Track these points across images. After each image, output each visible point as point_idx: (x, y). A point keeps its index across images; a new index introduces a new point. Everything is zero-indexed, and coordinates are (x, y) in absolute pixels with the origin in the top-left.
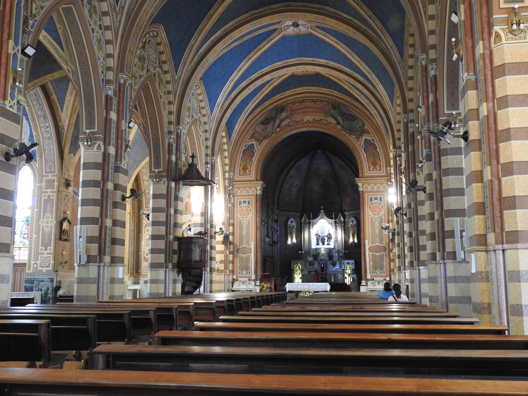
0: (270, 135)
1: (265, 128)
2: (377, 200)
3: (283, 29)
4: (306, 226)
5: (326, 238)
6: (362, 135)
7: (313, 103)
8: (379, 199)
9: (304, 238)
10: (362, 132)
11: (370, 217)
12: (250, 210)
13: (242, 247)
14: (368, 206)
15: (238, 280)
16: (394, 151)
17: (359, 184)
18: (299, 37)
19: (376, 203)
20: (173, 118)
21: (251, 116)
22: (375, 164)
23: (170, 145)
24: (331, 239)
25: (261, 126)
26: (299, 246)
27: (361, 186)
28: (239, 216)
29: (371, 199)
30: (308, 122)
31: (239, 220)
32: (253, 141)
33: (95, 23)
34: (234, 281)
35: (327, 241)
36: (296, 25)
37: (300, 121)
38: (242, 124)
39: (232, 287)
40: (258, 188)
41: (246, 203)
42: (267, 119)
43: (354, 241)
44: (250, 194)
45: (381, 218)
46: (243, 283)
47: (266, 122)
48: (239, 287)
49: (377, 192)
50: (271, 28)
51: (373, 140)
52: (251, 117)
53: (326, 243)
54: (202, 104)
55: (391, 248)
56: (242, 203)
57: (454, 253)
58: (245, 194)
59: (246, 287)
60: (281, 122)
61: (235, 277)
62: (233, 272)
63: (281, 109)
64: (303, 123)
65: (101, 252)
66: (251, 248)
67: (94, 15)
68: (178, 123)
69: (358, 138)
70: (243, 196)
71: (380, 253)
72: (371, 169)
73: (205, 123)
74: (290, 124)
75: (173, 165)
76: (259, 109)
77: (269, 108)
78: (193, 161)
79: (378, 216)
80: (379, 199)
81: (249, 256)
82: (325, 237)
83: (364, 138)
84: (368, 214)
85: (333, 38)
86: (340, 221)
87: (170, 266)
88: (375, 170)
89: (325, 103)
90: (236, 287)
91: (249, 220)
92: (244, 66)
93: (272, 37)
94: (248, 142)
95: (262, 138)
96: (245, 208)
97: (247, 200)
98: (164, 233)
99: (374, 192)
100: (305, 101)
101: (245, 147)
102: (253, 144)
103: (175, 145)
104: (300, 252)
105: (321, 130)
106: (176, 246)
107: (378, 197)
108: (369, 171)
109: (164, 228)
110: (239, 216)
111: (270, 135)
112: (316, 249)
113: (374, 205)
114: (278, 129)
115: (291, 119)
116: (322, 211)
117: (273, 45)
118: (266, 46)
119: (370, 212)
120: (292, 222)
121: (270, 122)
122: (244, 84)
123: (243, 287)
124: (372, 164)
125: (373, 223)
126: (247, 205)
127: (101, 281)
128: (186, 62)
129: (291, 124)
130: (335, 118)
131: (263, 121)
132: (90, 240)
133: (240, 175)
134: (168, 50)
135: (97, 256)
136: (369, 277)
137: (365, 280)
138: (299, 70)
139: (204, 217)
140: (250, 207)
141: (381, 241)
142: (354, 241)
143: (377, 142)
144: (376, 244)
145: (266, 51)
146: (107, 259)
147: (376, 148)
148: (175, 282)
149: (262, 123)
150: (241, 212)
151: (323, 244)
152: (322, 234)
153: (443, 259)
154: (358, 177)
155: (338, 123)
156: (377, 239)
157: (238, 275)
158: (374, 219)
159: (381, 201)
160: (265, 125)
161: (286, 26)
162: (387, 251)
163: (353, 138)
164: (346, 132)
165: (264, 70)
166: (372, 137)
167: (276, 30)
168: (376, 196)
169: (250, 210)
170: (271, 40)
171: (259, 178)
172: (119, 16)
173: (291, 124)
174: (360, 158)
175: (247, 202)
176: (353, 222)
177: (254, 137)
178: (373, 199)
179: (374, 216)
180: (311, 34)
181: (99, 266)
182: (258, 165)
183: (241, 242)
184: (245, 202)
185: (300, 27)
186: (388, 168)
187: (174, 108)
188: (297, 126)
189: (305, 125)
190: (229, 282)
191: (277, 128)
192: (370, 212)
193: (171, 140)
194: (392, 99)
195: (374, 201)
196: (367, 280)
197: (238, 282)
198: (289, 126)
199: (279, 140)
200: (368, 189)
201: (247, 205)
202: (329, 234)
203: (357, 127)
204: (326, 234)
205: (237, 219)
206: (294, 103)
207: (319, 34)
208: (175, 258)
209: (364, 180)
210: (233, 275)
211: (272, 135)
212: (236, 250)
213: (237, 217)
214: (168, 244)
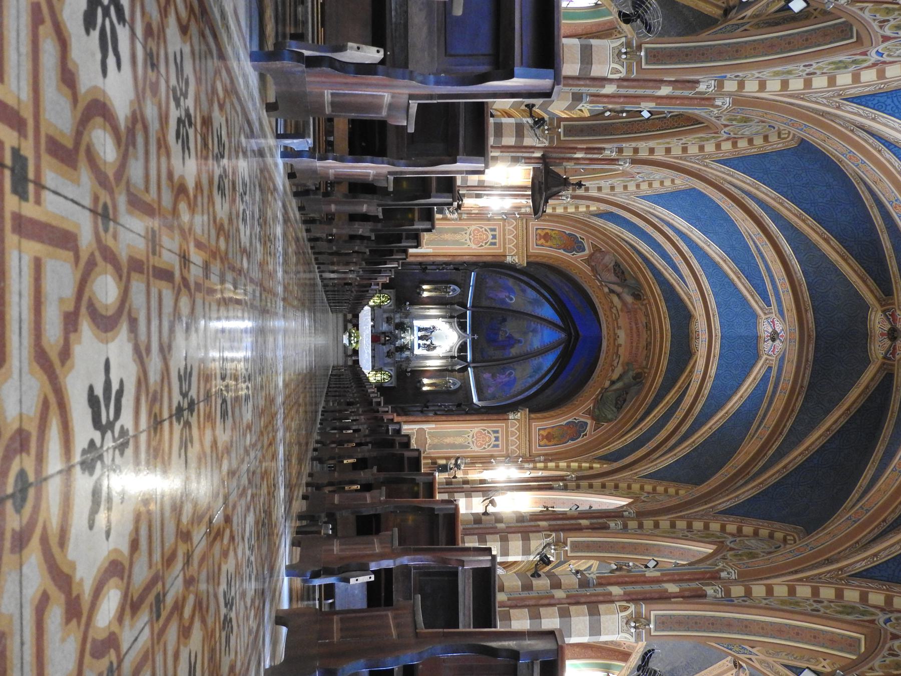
1: (609, 270)
2: (495, 441)
3: (768, 316)
4: (446, 312)
5: (428, 343)
6: (593, 418)
8: (497, 443)
9: (429, 309)
10: (598, 419)
11: (469, 430)
14: (485, 427)
16: (572, 477)
17: (519, 414)
18: (757, 338)
19: (490, 439)
21: (629, 247)
22: (549, 437)
24: (428, 350)
25: (613, 264)
26: (417, 300)
27: (516, 417)
29: (497, 432)
30: (616, 337)
35: (425, 344)
36: (774, 337)
38: (617, 235)
42: (623, 273)
45: (467, 447)
47: (619, 270)
49: (507, 440)
51: (586, 435)
52: (627, 248)
53: (421, 342)
60: (619, 295)
69: (589, 412)
72: (542, 432)
74: (614, 308)
79: (471, 443)
80: (497, 443)
82: (430, 341)
83: (589, 422)
84: (474, 427)
85: (750, 391)
86: (456, 365)
88: (540, 438)
93: (758, 297)
95: (593, 264)
99: (507, 436)
102: (584, 250)
104: (408, 303)
105: (603, 356)
107: (499, 443)
108: (539, 429)
112: (412, 328)
114: (606, 290)
115: (622, 310)
117: (744, 299)
118: (743, 286)
119: (476, 430)
121: (618, 277)
129: (614, 311)
130: (619, 379)
131: (619, 266)
149: (617, 265)
151: (420, 338)
152: (435, 337)
154: (531, 411)
158: (466, 436)
160: (615, 270)
161: (773, 322)
167: (769, 305)
170: (752, 296)
173: (614, 311)
174: (558, 416)
176: (454, 384)
178: (496, 435)
180: (757, 357)
185: (770, 342)
188: (610, 320)
189: (611, 333)
191: (609, 288)
192: (476, 430)
194: (651, 476)
195: (493, 436)
202: (435, 348)
203: (605, 410)
204: (435, 343)
207: (757, 371)
209: (525, 422)
211: (598, 280)
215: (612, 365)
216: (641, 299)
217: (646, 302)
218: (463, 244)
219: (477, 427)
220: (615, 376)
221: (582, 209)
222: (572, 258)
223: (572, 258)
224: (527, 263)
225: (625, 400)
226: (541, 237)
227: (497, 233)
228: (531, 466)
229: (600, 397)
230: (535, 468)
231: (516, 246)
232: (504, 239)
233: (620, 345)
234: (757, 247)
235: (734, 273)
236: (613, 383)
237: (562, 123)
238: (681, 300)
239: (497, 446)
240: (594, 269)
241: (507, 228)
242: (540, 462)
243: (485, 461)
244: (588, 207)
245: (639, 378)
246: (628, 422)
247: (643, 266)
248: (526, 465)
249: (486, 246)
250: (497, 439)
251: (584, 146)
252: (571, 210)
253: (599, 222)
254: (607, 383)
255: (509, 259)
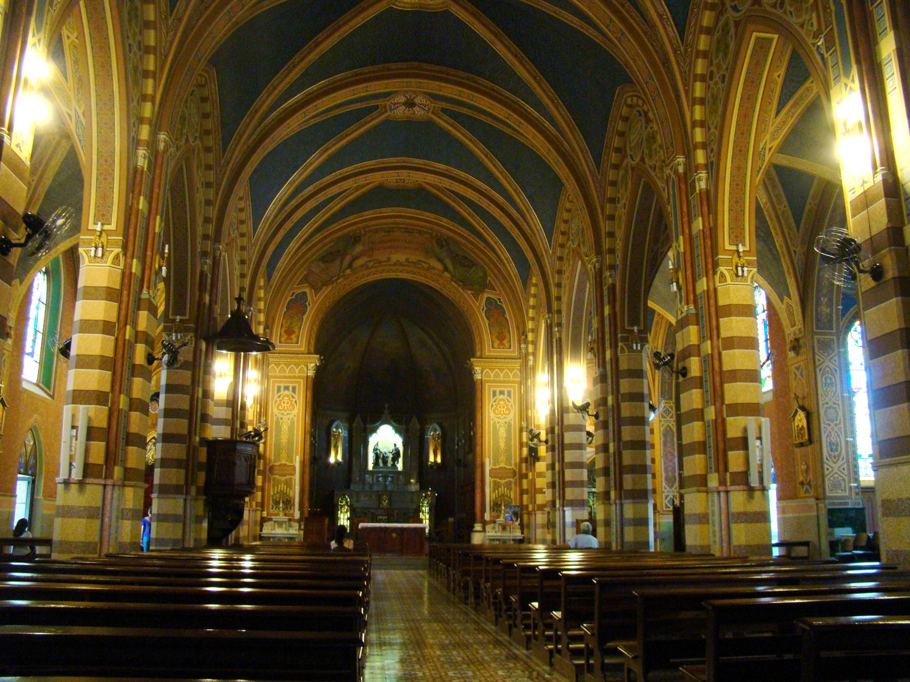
0: (334, 279)
2: (504, 394)
6: (482, 291)
7: (406, 235)
11: (492, 422)
12: (296, 402)
13: (278, 464)
14: (489, 404)
15: (270, 520)
17: (476, 368)
18: (409, 124)
19: (501, 400)
20: (211, 229)
21: (304, 247)
22: (501, 338)
23: (203, 275)
25: (321, 264)
27: (479, 371)
28: (275, 411)
29: (494, 393)
30: (398, 263)
31: (275, 418)
32: (304, 287)
33: (135, 34)
34: (263, 520)
37: (384, 262)
38: (291, 258)
39: (261, 530)
40: (310, 365)
41: (288, 390)
42: (331, 253)
43: (435, 461)
44: (297, 375)
45: (510, 425)
46: (280, 524)
47: (330, 257)
48: (273, 532)
49: (504, 382)
50: (372, 103)
52: (305, 248)
54: (243, 216)
55: (524, 471)
56: (282, 389)
57: (746, 474)
58: (287, 374)
59: (286, 532)
60: (355, 258)
61: (265, 514)
62: (262, 505)
63: (356, 239)
64: (390, 265)
65: (110, 457)
66: (294, 468)
67: (133, 23)
68: (217, 239)
70: (285, 377)
71: (507, 480)
72: (496, 345)
73: (243, 248)
75: (206, 311)
76: (319, 236)
77: (335, 236)
78: (239, 307)
81: (291, 479)
83: (486, 296)
84: (489, 417)
87: (193, 490)
88: (501, 347)
89: (426, 236)
90: (267, 530)
91: (293, 419)
92: (315, 160)
94: (297, 288)
95: (320, 284)
96: (286, 398)
97: (291, 385)
98: (186, 432)
99: (500, 382)
100: (395, 230)
101: (292, 296)
102: (305, 293)
103: (210, 276)
106: (203, 455)
107: (506, 390)
109: (185, 422)
110: (275, 411)
111: (334, 279)
113: (499, 403)
114: (348, 271)
116: (386, 411)
119: (492, 415)
120: (337, 427)
122: (311, 189)
123: (279, 531)
124: (498, 338)
125: (496, 431)
126: (290, 393)
127: (107, 514)
128: (241, 137)
131: (324, 257)
132: (92, 433)
133: (280, 342)
134: (217, 113)
135: (102, 465)
136: (487, 517)
137: (481, 523)
138: (390, 178)
139: (230, 409)
140: (296, 397)
141: (508, 460)
142: (435, 461)
143: (505, 302)
144: (501, 466)
145: (356, 140)
146: (118, 471)
147: (504, 313)
148: (199, 520)
149: (323, 259)
150: (280, 404)
153: (722, 482)
155: (446, 269)
156: (502, 458)
157: (271, 511)
158: (498, 425)
159: (510, 397)
162: (517, 476)
163: (468, 295)
164: (459, 285)
165: (345, 170)
166: (497, 295)
168: (502, 389)
169: (296, 402)
171: (312, 349)
172: (172, 33)
173: (370, 265)
174: (479, 327)
175: (291, 388)
177: (307, 282)
179: (499, 420)
181: (105, 486)
182: (312, 328)
183: (278, 456)
184: (286, 388)
186: (523, 346)
187: (213, 212)
190: (256, 522)
192: (492, 415)
193: (206, 268)
196: (484, 523)
197: (270, 523)
198: (368, 268)
199: (348, 288)
200: (490, 377)
201: (290, 393)
205: (272, 417)
206: (377, 231)
208: (202, 477)
209: (485, 362)
210: (263, 510)
212: (268, 468)
213: (272, 413)
214: (191, 451)
215: (428, 269)
216: (360, 237)
217: (363, 232)
218: (293, 422)
219: (489, 412)
220: (439, 266)
221: (262, 293)
222: (312, 308)
223: (312, 308)
224: (316, 353)
225: (465, 258)
226: (289, 338)
227: (282, 385)
228: (531, 358)
229: (461, 283)
230: (534, 354)
231: (297, 365)
232: (289, 377)
233: (407, 260)
234: (314, 117)
235: (340, 140)
236: (446, 269)
237: (171, 317)
238: (363, 195)
239: (509, 394)
240: (326, 284)
241: (277, 374)
242: (527, 348)
243: (525, 407)
244: (260, 288)
245: (443, 242)
246: (488, 257)
247: (325, 233)
248: (531, 363)
249: (296, 397)
250: (502, 393)
251: (197, 293)
252: (262, 305)
253: (277, 276)
254: (446, 274)
255: (311, 373)
